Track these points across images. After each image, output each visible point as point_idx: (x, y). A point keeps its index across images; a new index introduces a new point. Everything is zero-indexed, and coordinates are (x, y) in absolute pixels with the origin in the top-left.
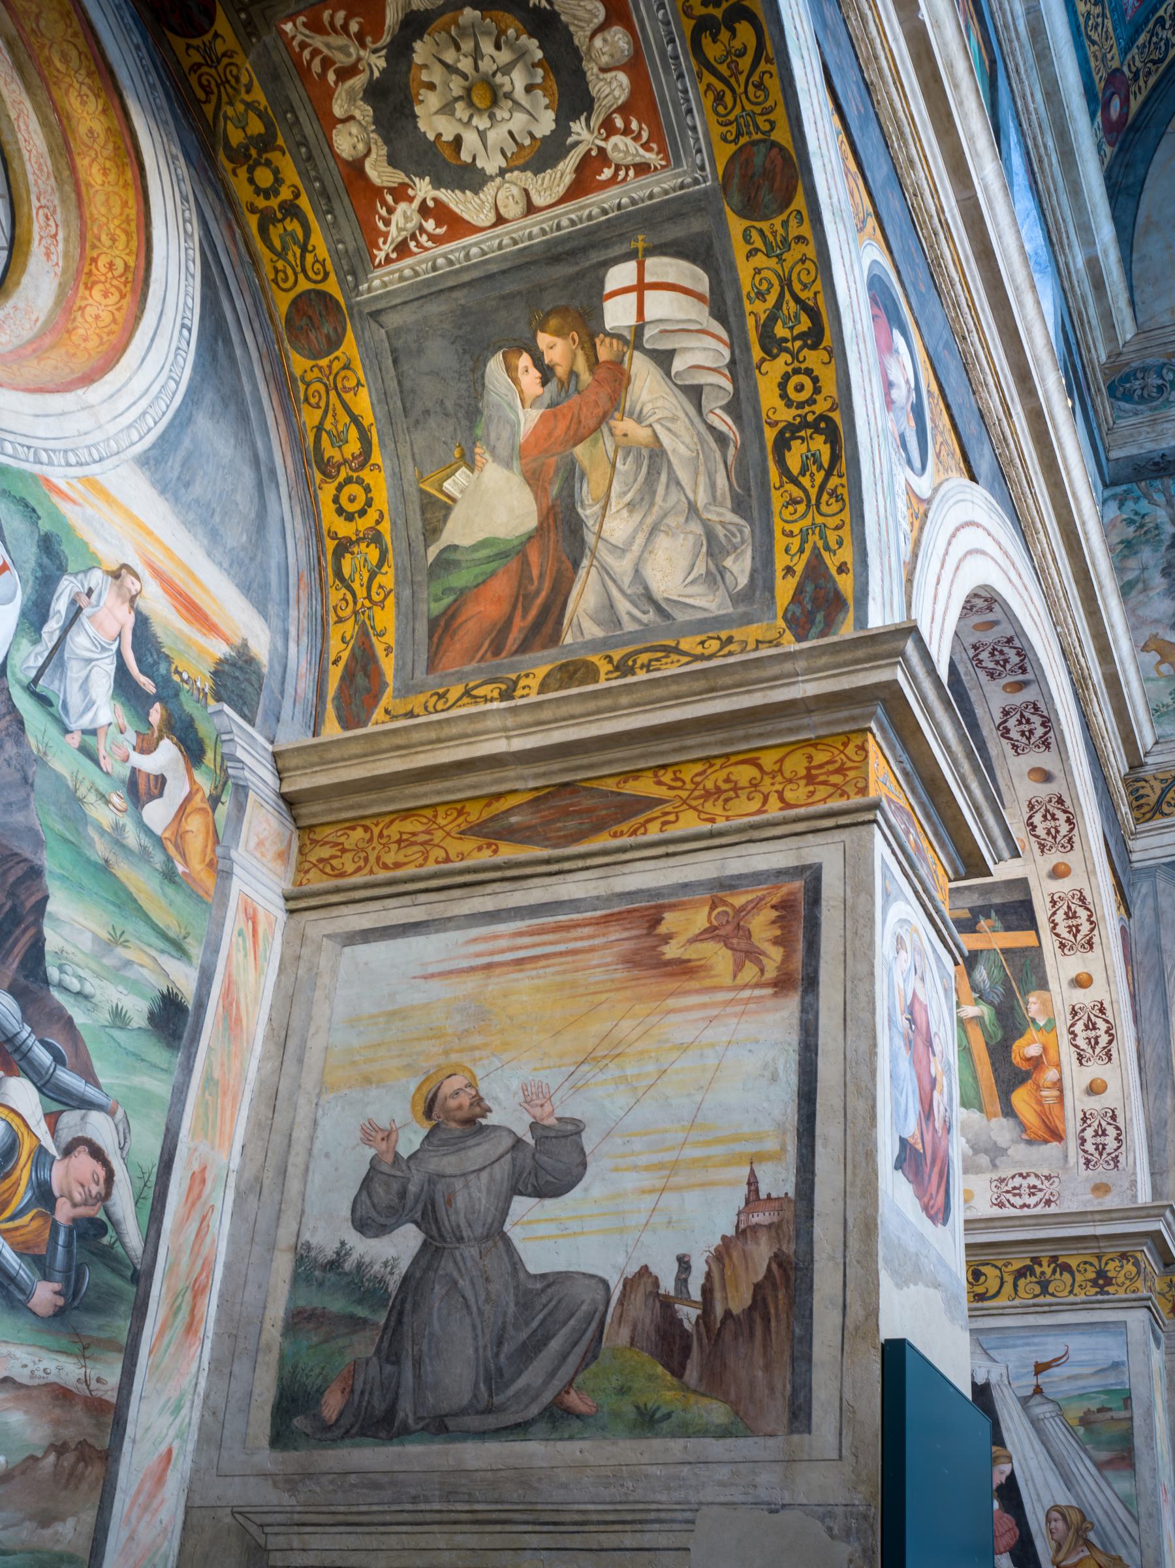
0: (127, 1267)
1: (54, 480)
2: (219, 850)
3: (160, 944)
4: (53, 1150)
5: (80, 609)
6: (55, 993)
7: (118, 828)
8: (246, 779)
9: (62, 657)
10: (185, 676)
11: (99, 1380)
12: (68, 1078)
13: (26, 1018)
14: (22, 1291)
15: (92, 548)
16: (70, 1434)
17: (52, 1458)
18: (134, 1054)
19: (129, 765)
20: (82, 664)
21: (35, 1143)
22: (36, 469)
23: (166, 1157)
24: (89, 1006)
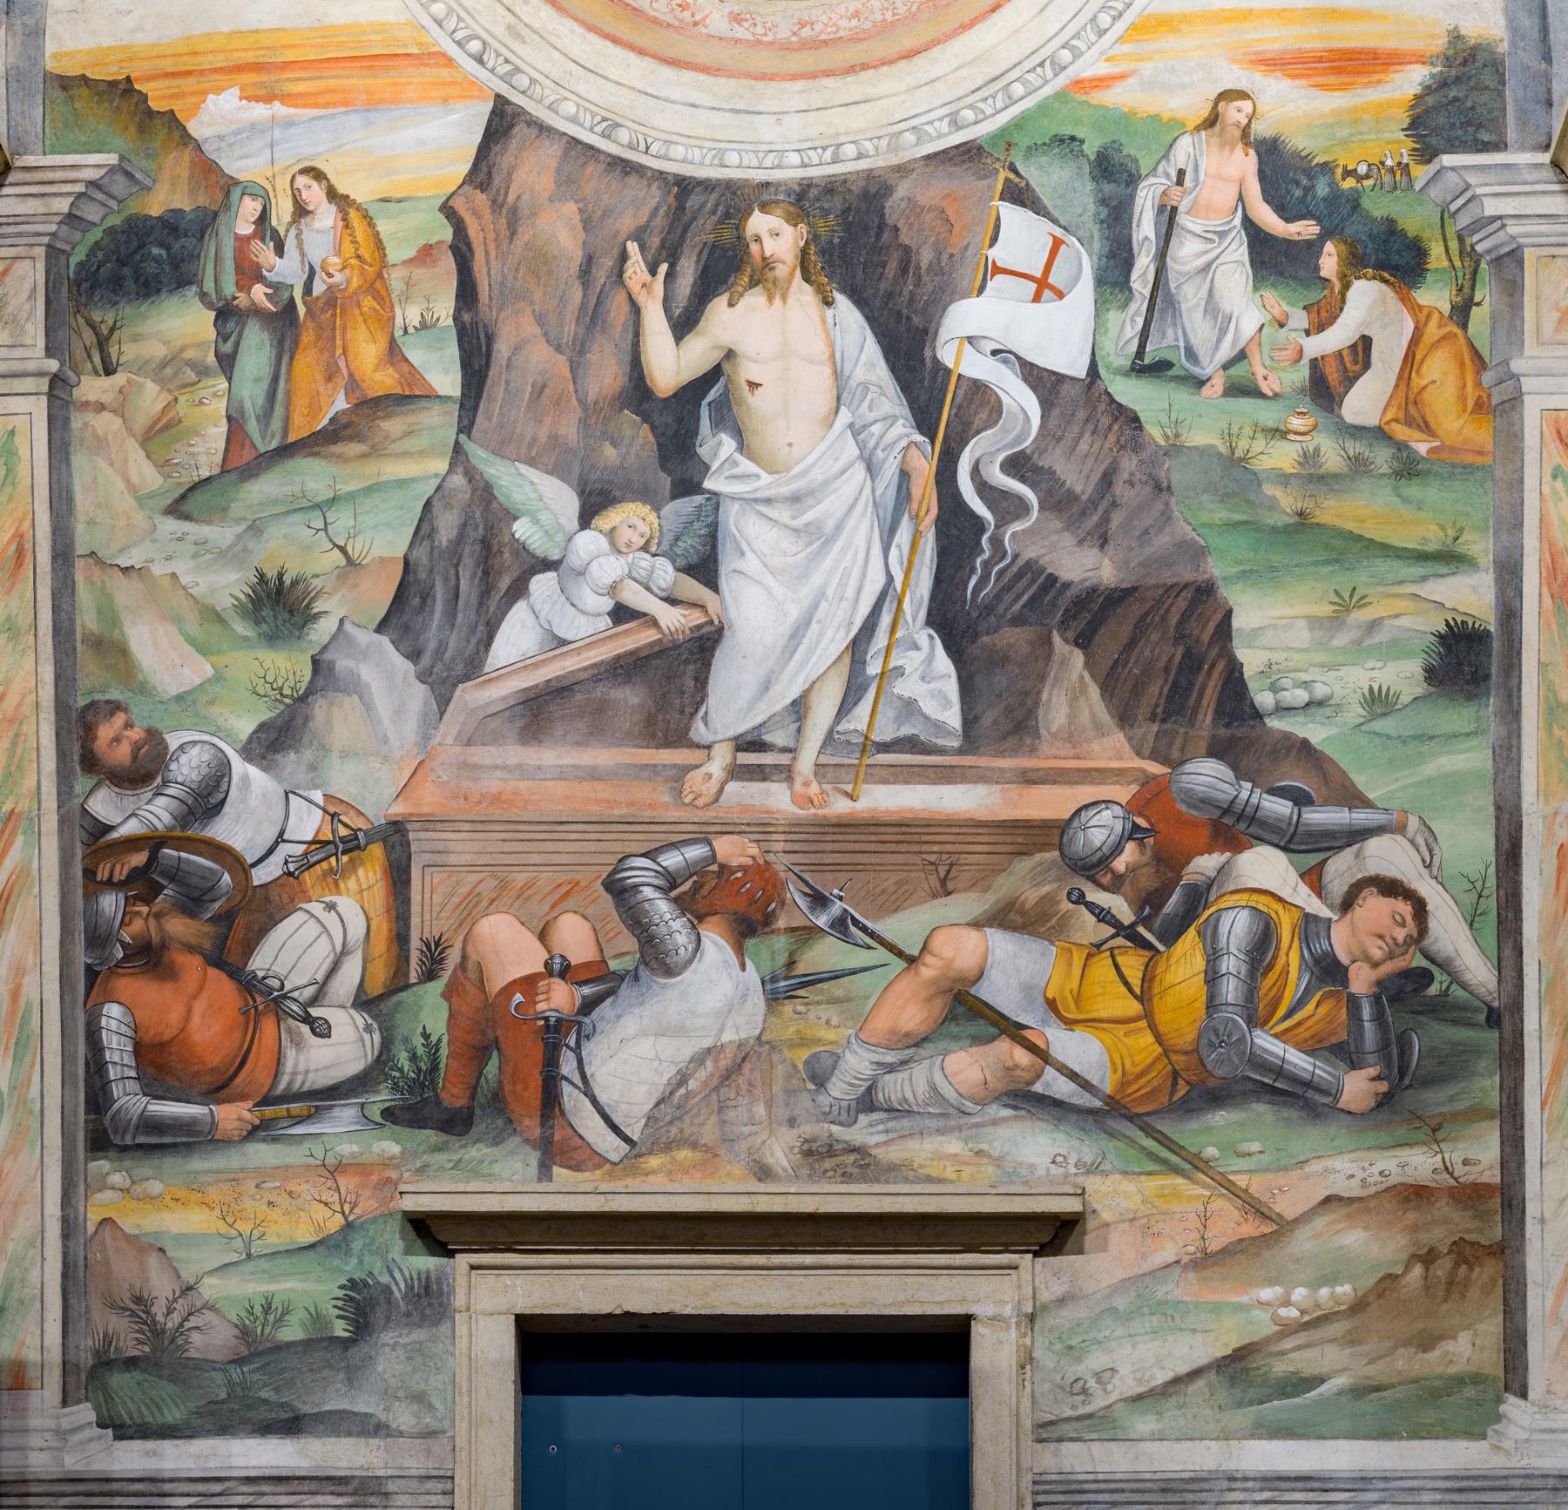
0: (1477, 1010)
1: (1088, 74)
2: (1488, 378)
3: (1417, 570)
4: (1324, 912)
5: (1174, 209)
6: (1274, 723)
7: (1310, 458)
8: (1513, 238)
9: (1168, 294)
10: (1362, 169)
11: (1465, 1162)
12: (1321, 816)
13: (1240, 774)
14: (1325, 1092)
15: (1166, 116)
16: (1438, 1237)
17: (1418, 1270)
18: (1415, 737)
19: (1305, 361)
20: (1199, 279)
21: (1296, 914)
22: (1062, 80)
23: (1506, 845)
24: (1328, 711)
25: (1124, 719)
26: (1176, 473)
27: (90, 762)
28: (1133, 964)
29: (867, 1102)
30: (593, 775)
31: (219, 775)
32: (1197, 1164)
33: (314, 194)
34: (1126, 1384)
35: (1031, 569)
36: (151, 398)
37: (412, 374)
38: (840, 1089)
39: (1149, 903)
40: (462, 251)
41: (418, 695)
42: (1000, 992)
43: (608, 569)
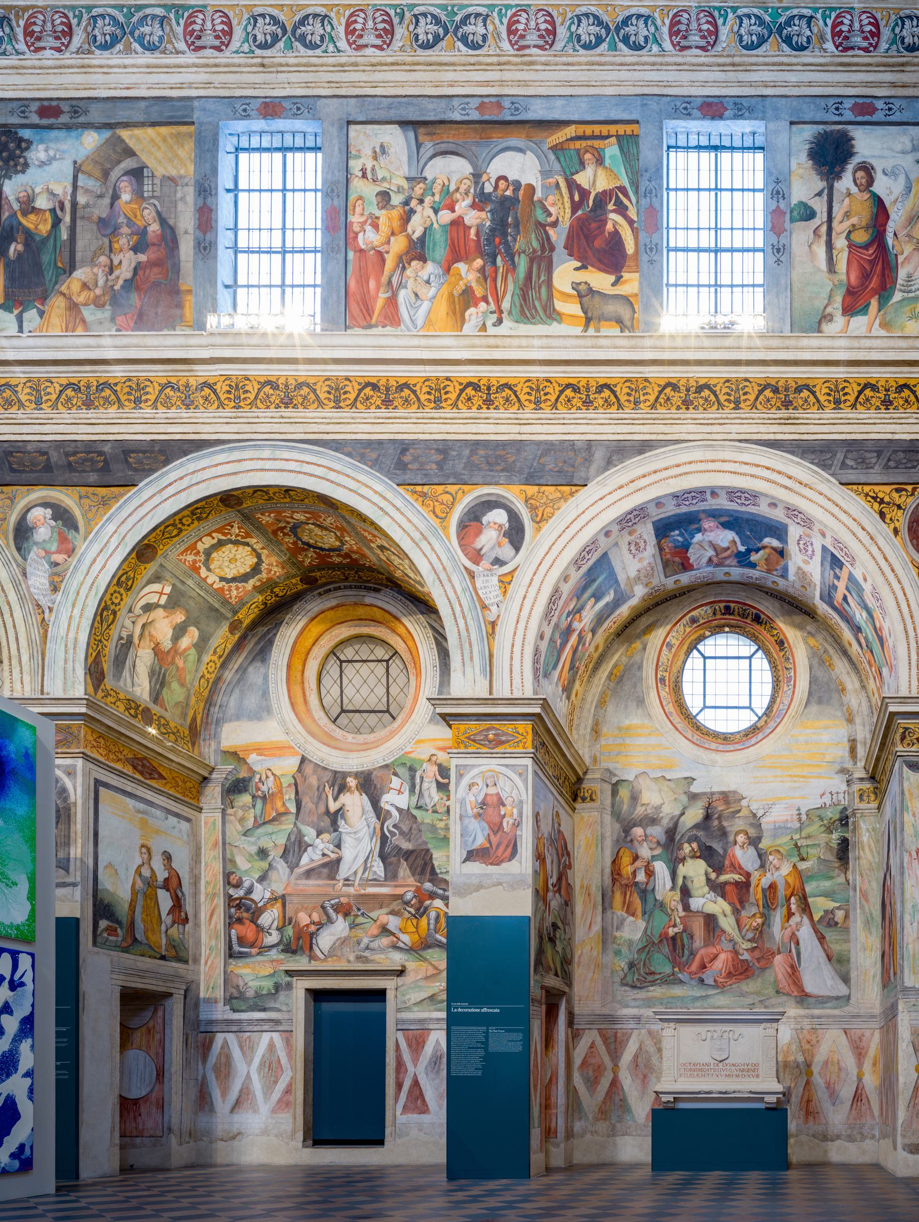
25: (413, 875)
26: (423, 828)
27: (229, 883)
28: (415, 921)
29: (367, 948)
30: (319, 886)
31: (252, 886)
32: (426, 960)
33: (269, 774)
34: (413, 1001)
35: (397, 846)
36: (240, 813)
37: (287, 809)
38: (362, 945)
39: (418, 910)
40: (296, 785)
41: (288, 870)
42: (391, 927)
43: (321, 846)
